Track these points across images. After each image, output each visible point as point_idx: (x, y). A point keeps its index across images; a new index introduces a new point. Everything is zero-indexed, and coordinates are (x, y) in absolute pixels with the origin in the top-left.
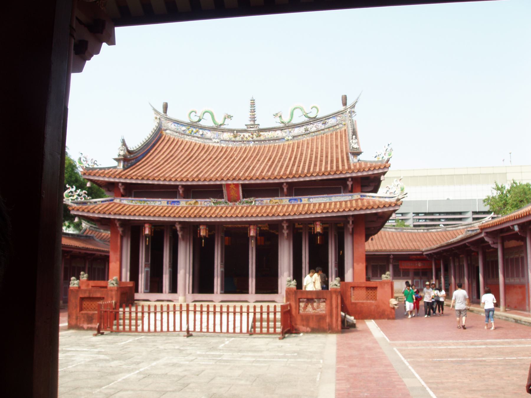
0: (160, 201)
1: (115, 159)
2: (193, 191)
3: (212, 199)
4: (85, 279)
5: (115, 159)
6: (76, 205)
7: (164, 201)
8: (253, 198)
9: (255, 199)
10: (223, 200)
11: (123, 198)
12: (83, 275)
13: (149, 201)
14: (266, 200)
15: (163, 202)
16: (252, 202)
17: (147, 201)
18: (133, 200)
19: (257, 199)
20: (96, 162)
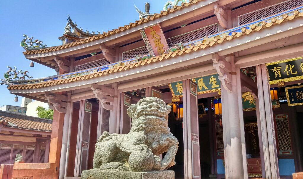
0: (92, 71)
1: (60, 38)
2: (123, 54)
3: (136, 56)
4: (18, 161)
5: (60, 38)
6: (14, 85)
7: (95, 69)
8: (180, 43)
9: (183, 44)
10: (148, 54)
11: (63, 75)
12: (18, 157)
13: (83, 73)
14: (198, 43)
15: (94, 71)
16: (180, 48)
17: (82, 73)
18: (71, 75)
19: (185, 44)
20: (41, 43)
